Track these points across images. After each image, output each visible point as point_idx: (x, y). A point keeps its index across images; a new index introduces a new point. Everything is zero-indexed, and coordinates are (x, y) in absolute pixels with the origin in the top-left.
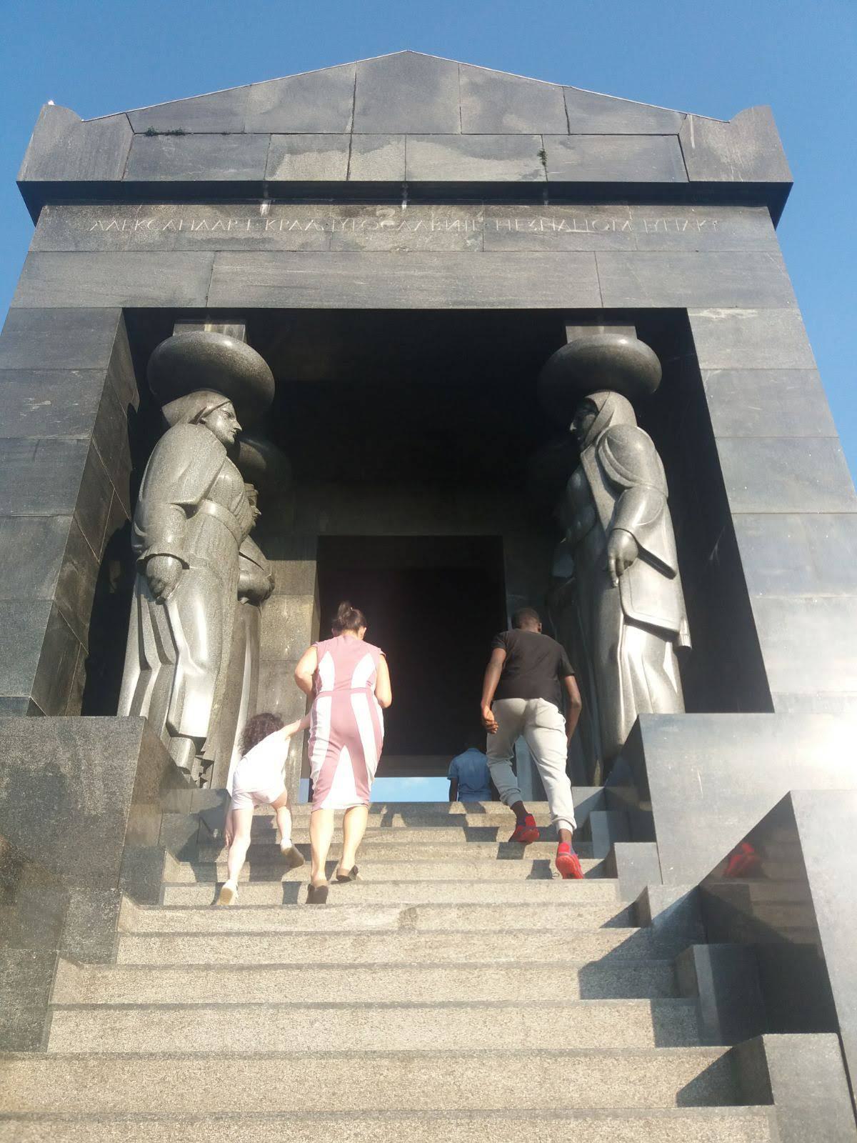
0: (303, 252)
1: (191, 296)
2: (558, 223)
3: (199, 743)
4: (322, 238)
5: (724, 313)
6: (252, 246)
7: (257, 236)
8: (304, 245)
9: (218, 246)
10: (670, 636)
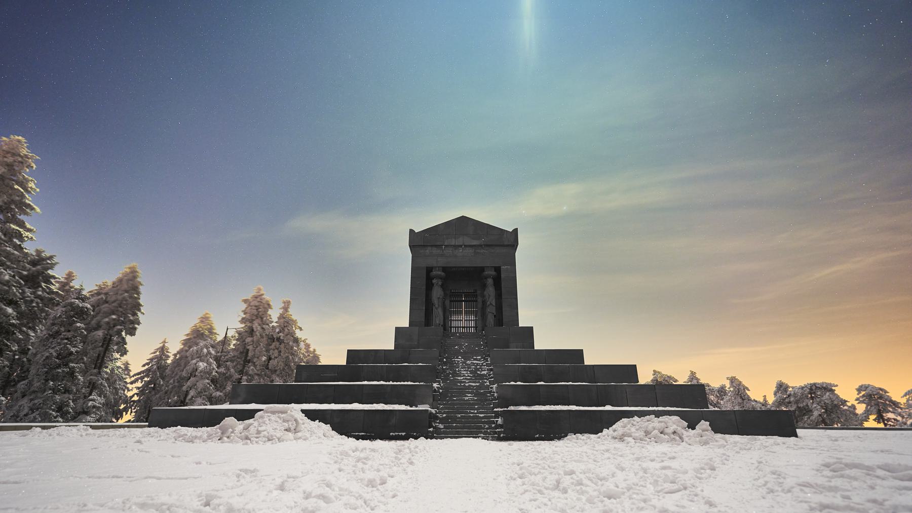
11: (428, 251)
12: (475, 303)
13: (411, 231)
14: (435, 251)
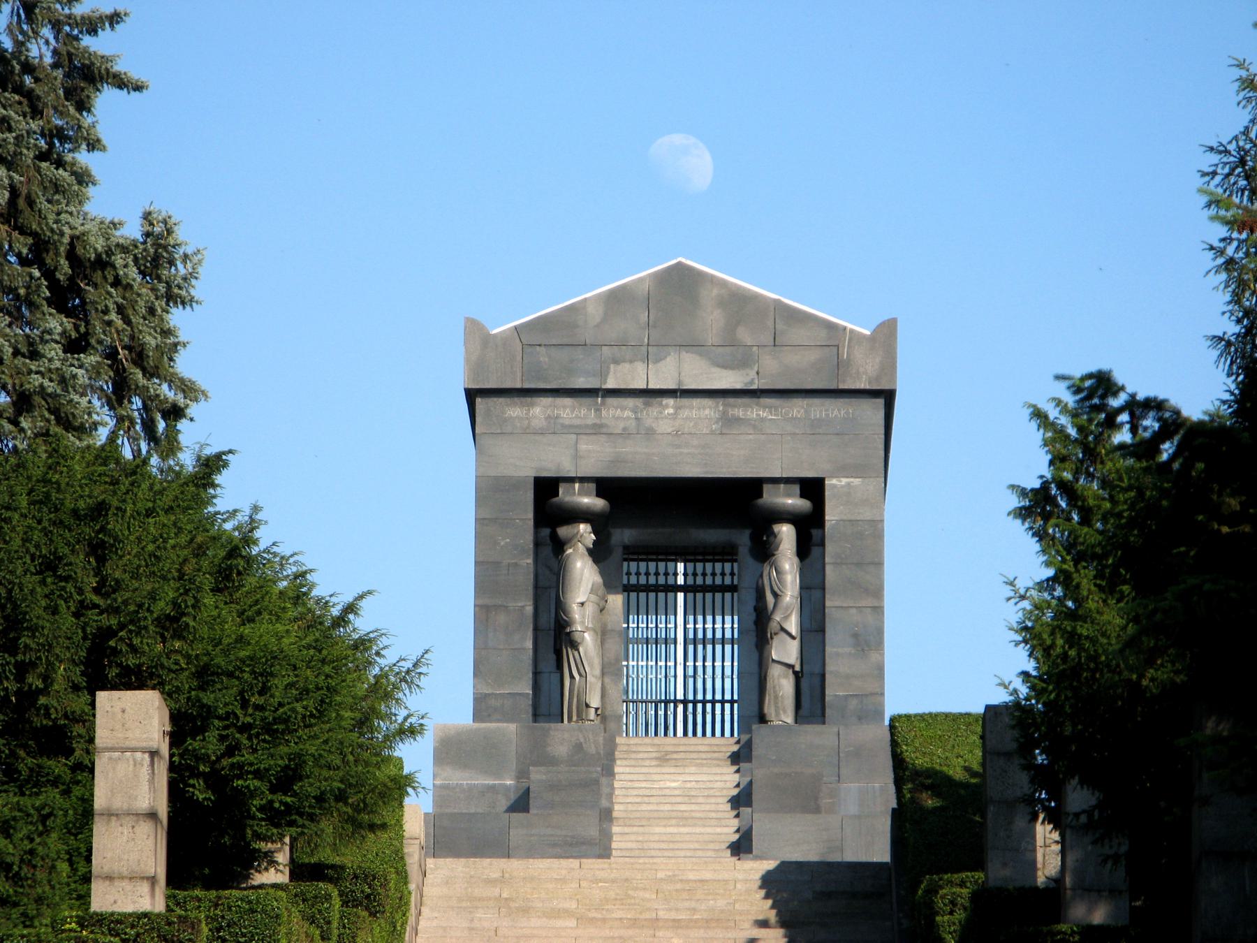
0: (625, 434)
1: (568, 469)
2: (763, 412)
3: (597, 709)
4: (634, 423)
5: (844, 481)
6: (597, 430)
7: (598, 422)
8: (624, 429)
9: (579, 431)
10: (792, 667)
11: (540, 409)
12: (728, 595)
13: (473, 328)
14: (567, 410)
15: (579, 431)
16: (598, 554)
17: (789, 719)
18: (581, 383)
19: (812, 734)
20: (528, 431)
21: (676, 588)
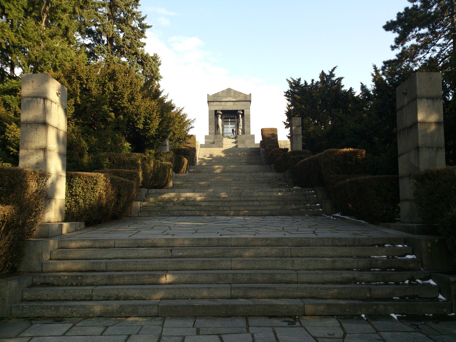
0: (224, 106)
6: (221, 105)
9: (219, 105)
11: (215, 103)
13: (208, 95)
14: (218, 103)
15: (219, 105)
16: (221, 118)
17: (241, 134)
18: (219, 100)
19: (244, 136)
20: (214, 105)
21: (229, 122)
